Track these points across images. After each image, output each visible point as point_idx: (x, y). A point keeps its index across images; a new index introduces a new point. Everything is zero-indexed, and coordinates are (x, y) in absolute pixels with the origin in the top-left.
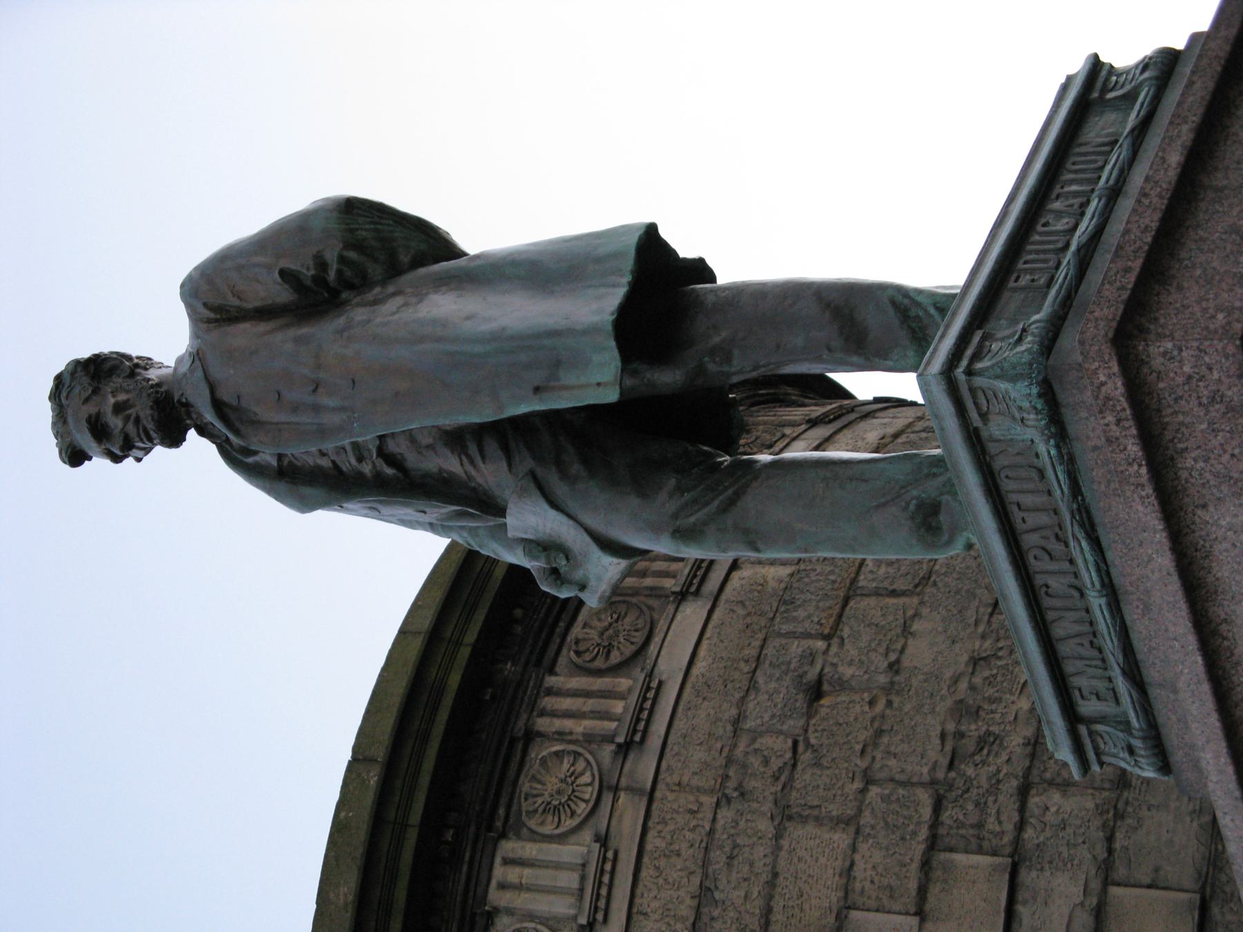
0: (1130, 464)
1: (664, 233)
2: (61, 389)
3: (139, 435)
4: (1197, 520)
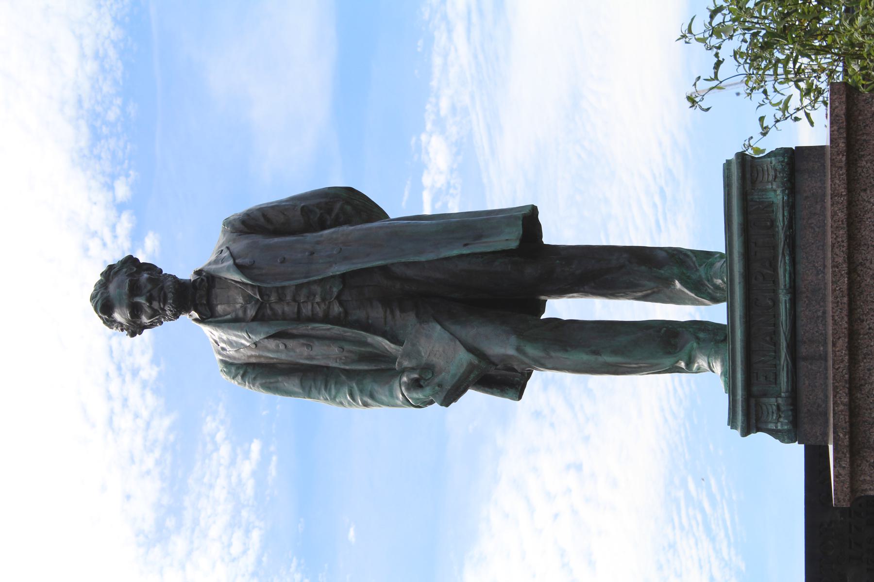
0: (838, 155)
1: (541, 218)
2: (110, 273)
3: (159, 297)
4: (860, 198)
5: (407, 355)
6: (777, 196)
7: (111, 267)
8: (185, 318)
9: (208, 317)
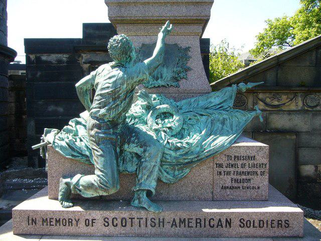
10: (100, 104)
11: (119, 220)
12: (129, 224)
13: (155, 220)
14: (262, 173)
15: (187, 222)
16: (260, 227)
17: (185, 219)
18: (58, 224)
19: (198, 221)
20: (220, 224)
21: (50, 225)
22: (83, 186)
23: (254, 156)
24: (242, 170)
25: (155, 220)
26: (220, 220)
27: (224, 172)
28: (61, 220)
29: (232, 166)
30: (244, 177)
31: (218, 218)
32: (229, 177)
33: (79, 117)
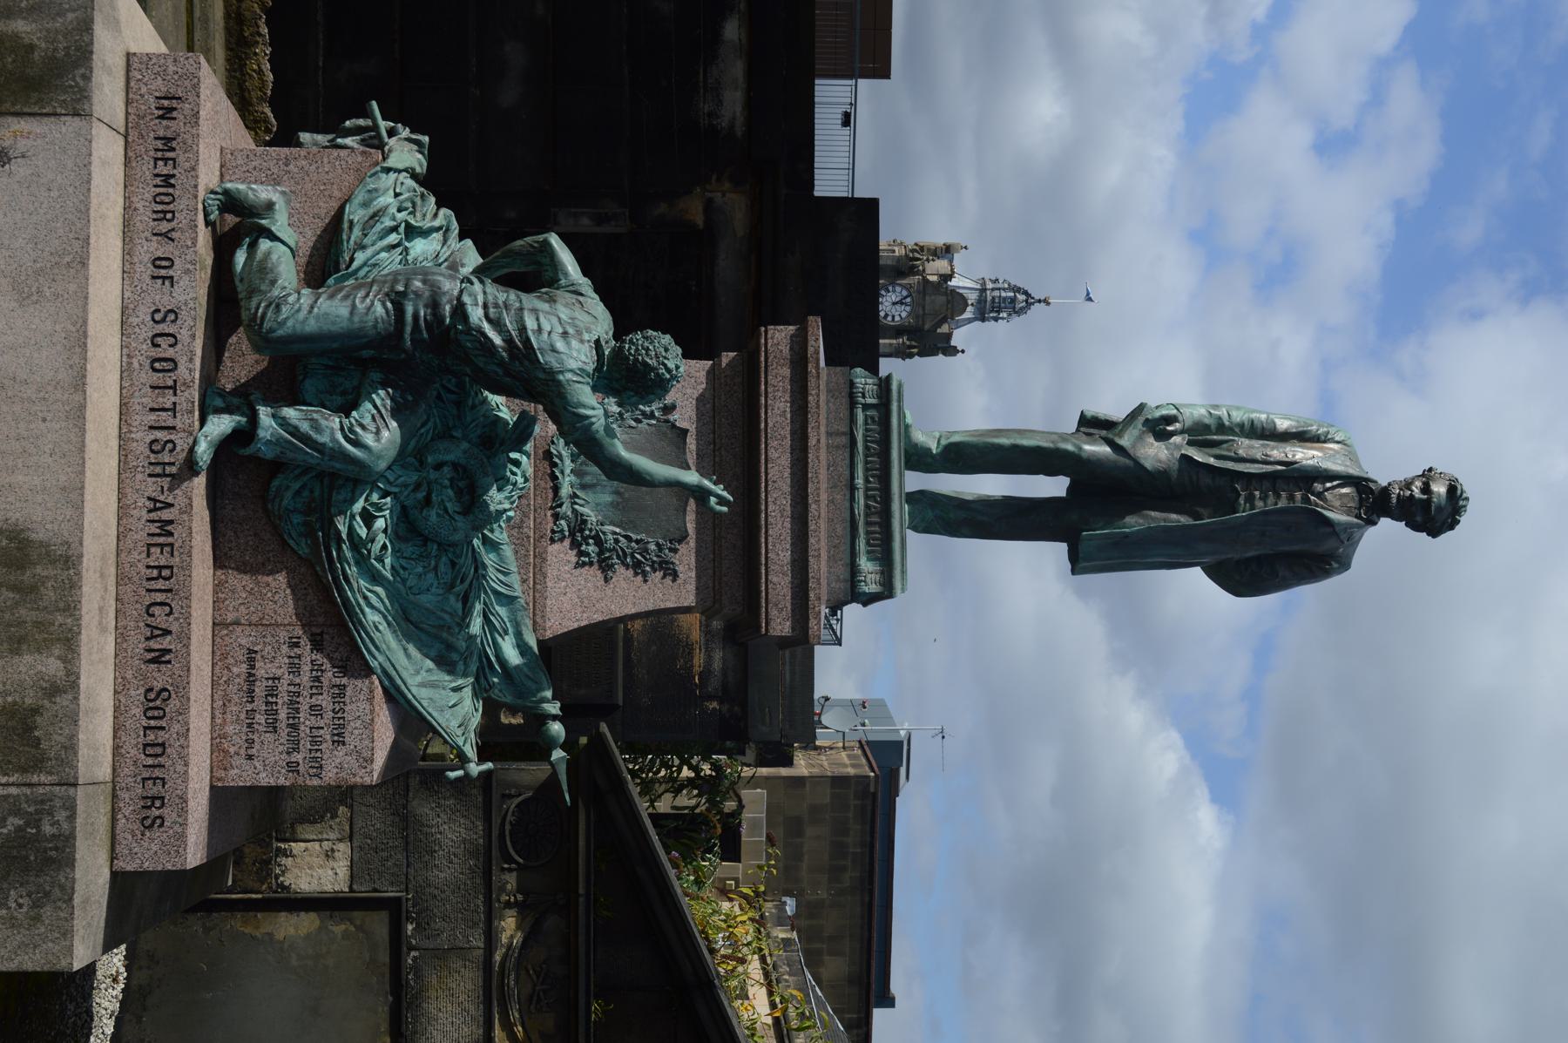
5: (1178, 447)
6: (866, 565)
7: (1452, 527)
8: (1384, 484)
9: (1360, 483)
10: (496, 306)
11: (170, 353)
12: (157, 378)
13: (171, 451)
14: (293, 767)
15: (161, 540)
16: (145, 746)
17: (171, 534)
18: (158, 181)
19: (166, 573)
20: (157, 632)
21: (156, 159)
22: (268, 254)
23: (344, 743)
24: (304, 707)
25: (171, 451)
26: (167, 632)
27: (299, 657)
28: (171, 190)
29: (317, 679)
30: (283, 715)
31: (174, 628)
32: (284, 670)
33: (462, 237)
